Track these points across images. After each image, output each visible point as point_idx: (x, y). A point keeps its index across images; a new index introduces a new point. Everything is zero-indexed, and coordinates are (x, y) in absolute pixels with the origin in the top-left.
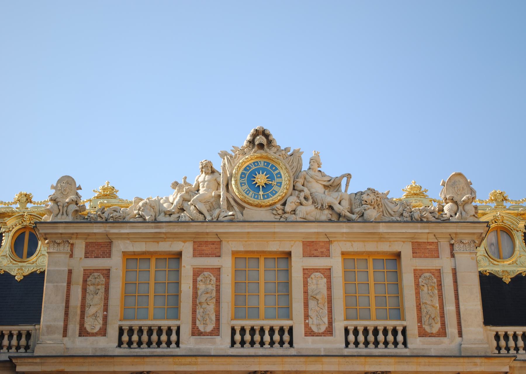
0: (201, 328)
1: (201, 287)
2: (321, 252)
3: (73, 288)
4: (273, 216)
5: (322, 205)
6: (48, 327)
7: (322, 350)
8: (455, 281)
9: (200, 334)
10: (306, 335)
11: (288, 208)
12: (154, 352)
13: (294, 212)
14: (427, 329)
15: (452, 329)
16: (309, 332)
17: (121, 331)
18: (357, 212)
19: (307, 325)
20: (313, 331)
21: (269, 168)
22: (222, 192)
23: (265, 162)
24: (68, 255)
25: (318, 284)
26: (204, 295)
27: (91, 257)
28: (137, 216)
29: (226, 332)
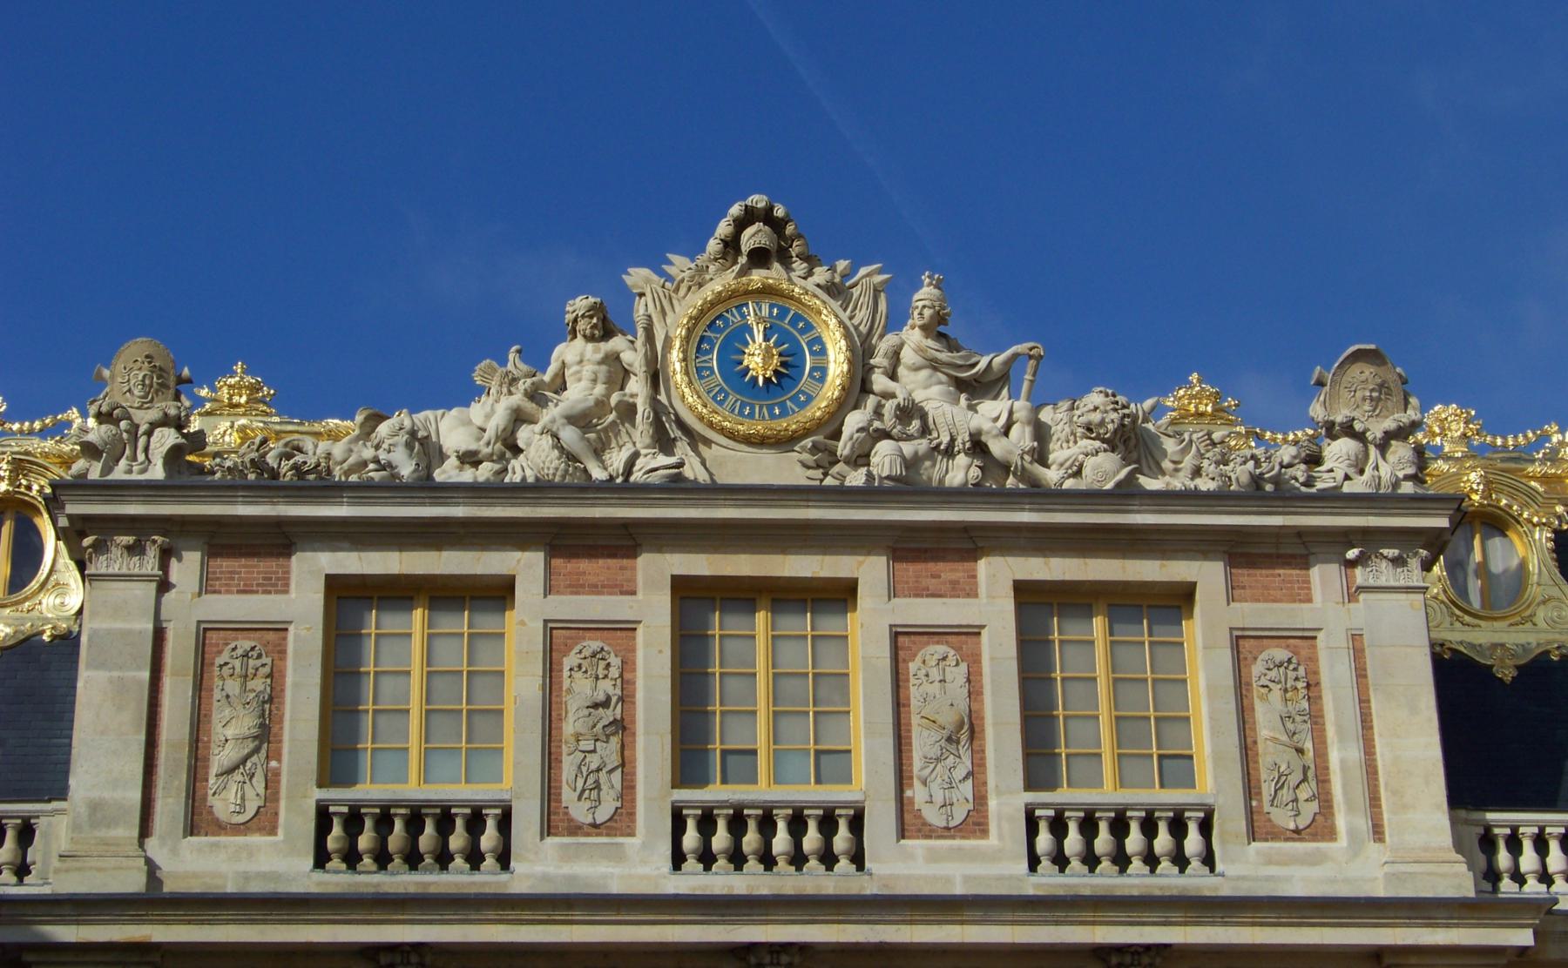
0: (580, 812)
1: (579, 689)
2: (951, 582)
3: (167, 682)
4: (799, 469)
5: (953, 440)
6: (95, 807)
7: (958, 880)
8: (1361, 674)
9: (575, 829)
11: (843, 448)
12: (430, 884)
17: (323, 818)
18: (1061, 459)
20: (925, 824)
21: (785, 324)
23: (772, 306)
24: (154, 585)
26: (586, 712)
27: (228, 592)
28: (371, 466)
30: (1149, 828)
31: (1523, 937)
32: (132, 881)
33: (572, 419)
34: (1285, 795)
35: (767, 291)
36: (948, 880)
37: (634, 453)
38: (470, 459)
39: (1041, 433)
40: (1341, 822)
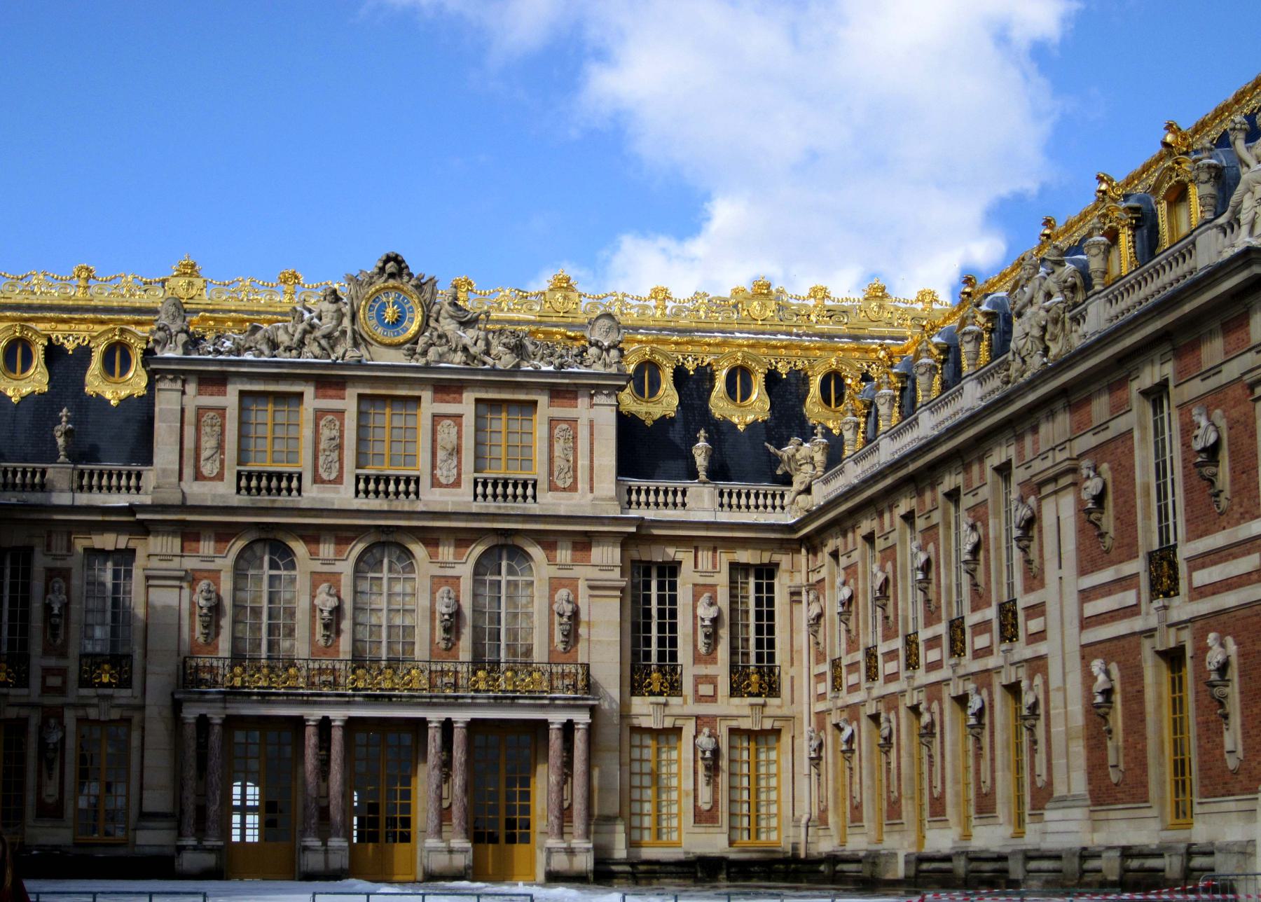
0: (325, 476)
1: (326, 433)
3: (186, 428)
6: (164, 471)
8: (592, 434)
9: (323, 482)
10: (433, 486)
11: (419, 349)
13: (424, 353)
14: (560, 484)
15: (582, 484)
16: (435, 483)
19: (433, 476)
22: (346, 322)
25: (447, 434)
29: (349, 480)
30: (515, 486)
31: (633, 529)
32: (175, 499)
33: (324, 337)
34: (562, 476)
35: (394, 288)
36: (446, 503)
37: (345, 351)
38: (288, 349)
39: (488, 344)
40: (579, 486)
